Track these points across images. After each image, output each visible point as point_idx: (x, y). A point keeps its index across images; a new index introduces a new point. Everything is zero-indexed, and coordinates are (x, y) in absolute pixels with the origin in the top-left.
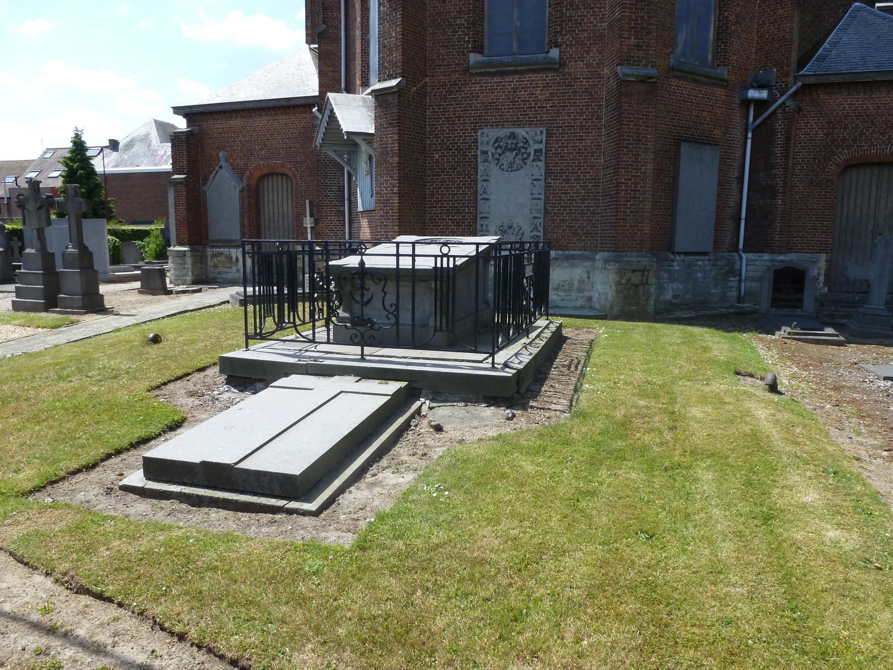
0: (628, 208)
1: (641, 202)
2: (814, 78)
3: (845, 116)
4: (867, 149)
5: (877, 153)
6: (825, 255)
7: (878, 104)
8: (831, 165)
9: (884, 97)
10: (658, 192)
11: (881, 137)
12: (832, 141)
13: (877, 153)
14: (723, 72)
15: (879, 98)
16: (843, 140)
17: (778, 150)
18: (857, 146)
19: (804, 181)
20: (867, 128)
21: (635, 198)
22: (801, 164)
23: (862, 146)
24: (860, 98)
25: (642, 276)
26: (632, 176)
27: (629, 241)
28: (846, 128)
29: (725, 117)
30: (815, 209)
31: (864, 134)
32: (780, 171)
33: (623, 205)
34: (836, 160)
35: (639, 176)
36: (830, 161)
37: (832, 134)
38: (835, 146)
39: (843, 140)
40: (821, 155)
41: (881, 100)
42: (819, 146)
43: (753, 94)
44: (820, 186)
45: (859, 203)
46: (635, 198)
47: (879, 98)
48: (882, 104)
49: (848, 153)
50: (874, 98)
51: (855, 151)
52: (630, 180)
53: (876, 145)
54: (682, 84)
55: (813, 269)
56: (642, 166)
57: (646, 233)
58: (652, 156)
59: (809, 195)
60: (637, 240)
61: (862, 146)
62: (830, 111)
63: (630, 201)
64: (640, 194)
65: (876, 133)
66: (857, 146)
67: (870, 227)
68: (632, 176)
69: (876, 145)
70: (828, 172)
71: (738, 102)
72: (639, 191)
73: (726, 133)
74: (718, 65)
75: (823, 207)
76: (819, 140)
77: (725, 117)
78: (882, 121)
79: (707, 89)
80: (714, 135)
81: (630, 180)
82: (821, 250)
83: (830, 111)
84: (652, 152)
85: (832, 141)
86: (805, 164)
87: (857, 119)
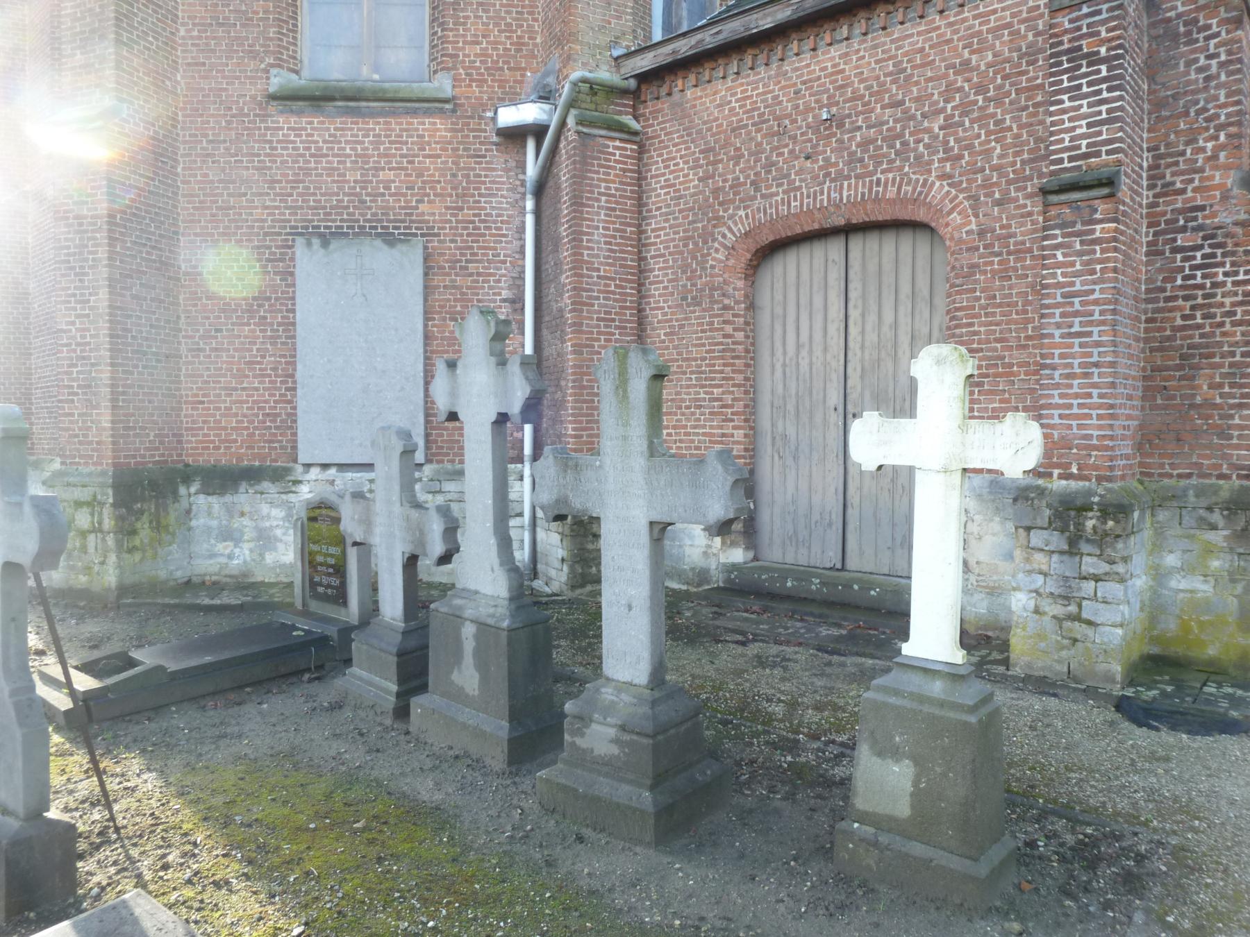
0: (73, 380)
1: (93, 365)
2: (651, 55)
3: (733, 130)
4: (783, 199)
5: (802, 205)
7: (795, 84)
8: (717, 250)
9: (808, 65)
10: (255, 343)
11: (808, 164)
12: (716, 191)
13: (802, 205)
14: (443, 85)
15: (797, 69)
16: (736, 185)
17: (563, 230)
18: (763, 196)
19: (672, 294)
20: (777, 148)
21: (84, 358)
22: (663, 255)
23: (773, 195)
24: (756, 82)
25: (92, 515)
26: (78, 316)
27: (80, 443)
28: (737, 158)
29: (454, 175)
30: (695, 359)
31: (773, 164)
32: (567, 277)
33: (66, 373)
34: (724, 236)
35: (88, 316)
36: (714, 240)
37: (713, 177)
38: (720, 204)
39: (736, 185)
40: (695, 229)
41: (802, 75)
42: (692, 209)
43: (509, 116)
44: (699, 304)
46: (84, 358)
47: (797, 69)
48: (804, 83)
49: (747, 215)
50: (787, 71)
51: (759, 209)
52: (73, 323)
53: (800, 188)
54: (311, 123)
56: (90, 294)
57: (104, 429)
58: (104, 273)
59: (682, 326)
60: (91, 443)
61: (773, 195)
62: (705, 123)
63: (75, 365)
64: (91, 350)
65: (797, 158)
66: (763, 196)
67: (834, 398)
68: (78, 316)
69: (800, 188)
70: (713, 267)
71: (495, 139)
72: (89, 344)
73: (461, 209)
74: (435, 72)
75: (707, 352)
76: (692, 195)
77: (454, 175)
78: (808, 126)
79: (386, 123)
80: (423, 214)
81: (73, 323)
83: (705, 123)
84: (106, 266)
85: (716, 191)
86: (670, 254)
87: (758, 131)
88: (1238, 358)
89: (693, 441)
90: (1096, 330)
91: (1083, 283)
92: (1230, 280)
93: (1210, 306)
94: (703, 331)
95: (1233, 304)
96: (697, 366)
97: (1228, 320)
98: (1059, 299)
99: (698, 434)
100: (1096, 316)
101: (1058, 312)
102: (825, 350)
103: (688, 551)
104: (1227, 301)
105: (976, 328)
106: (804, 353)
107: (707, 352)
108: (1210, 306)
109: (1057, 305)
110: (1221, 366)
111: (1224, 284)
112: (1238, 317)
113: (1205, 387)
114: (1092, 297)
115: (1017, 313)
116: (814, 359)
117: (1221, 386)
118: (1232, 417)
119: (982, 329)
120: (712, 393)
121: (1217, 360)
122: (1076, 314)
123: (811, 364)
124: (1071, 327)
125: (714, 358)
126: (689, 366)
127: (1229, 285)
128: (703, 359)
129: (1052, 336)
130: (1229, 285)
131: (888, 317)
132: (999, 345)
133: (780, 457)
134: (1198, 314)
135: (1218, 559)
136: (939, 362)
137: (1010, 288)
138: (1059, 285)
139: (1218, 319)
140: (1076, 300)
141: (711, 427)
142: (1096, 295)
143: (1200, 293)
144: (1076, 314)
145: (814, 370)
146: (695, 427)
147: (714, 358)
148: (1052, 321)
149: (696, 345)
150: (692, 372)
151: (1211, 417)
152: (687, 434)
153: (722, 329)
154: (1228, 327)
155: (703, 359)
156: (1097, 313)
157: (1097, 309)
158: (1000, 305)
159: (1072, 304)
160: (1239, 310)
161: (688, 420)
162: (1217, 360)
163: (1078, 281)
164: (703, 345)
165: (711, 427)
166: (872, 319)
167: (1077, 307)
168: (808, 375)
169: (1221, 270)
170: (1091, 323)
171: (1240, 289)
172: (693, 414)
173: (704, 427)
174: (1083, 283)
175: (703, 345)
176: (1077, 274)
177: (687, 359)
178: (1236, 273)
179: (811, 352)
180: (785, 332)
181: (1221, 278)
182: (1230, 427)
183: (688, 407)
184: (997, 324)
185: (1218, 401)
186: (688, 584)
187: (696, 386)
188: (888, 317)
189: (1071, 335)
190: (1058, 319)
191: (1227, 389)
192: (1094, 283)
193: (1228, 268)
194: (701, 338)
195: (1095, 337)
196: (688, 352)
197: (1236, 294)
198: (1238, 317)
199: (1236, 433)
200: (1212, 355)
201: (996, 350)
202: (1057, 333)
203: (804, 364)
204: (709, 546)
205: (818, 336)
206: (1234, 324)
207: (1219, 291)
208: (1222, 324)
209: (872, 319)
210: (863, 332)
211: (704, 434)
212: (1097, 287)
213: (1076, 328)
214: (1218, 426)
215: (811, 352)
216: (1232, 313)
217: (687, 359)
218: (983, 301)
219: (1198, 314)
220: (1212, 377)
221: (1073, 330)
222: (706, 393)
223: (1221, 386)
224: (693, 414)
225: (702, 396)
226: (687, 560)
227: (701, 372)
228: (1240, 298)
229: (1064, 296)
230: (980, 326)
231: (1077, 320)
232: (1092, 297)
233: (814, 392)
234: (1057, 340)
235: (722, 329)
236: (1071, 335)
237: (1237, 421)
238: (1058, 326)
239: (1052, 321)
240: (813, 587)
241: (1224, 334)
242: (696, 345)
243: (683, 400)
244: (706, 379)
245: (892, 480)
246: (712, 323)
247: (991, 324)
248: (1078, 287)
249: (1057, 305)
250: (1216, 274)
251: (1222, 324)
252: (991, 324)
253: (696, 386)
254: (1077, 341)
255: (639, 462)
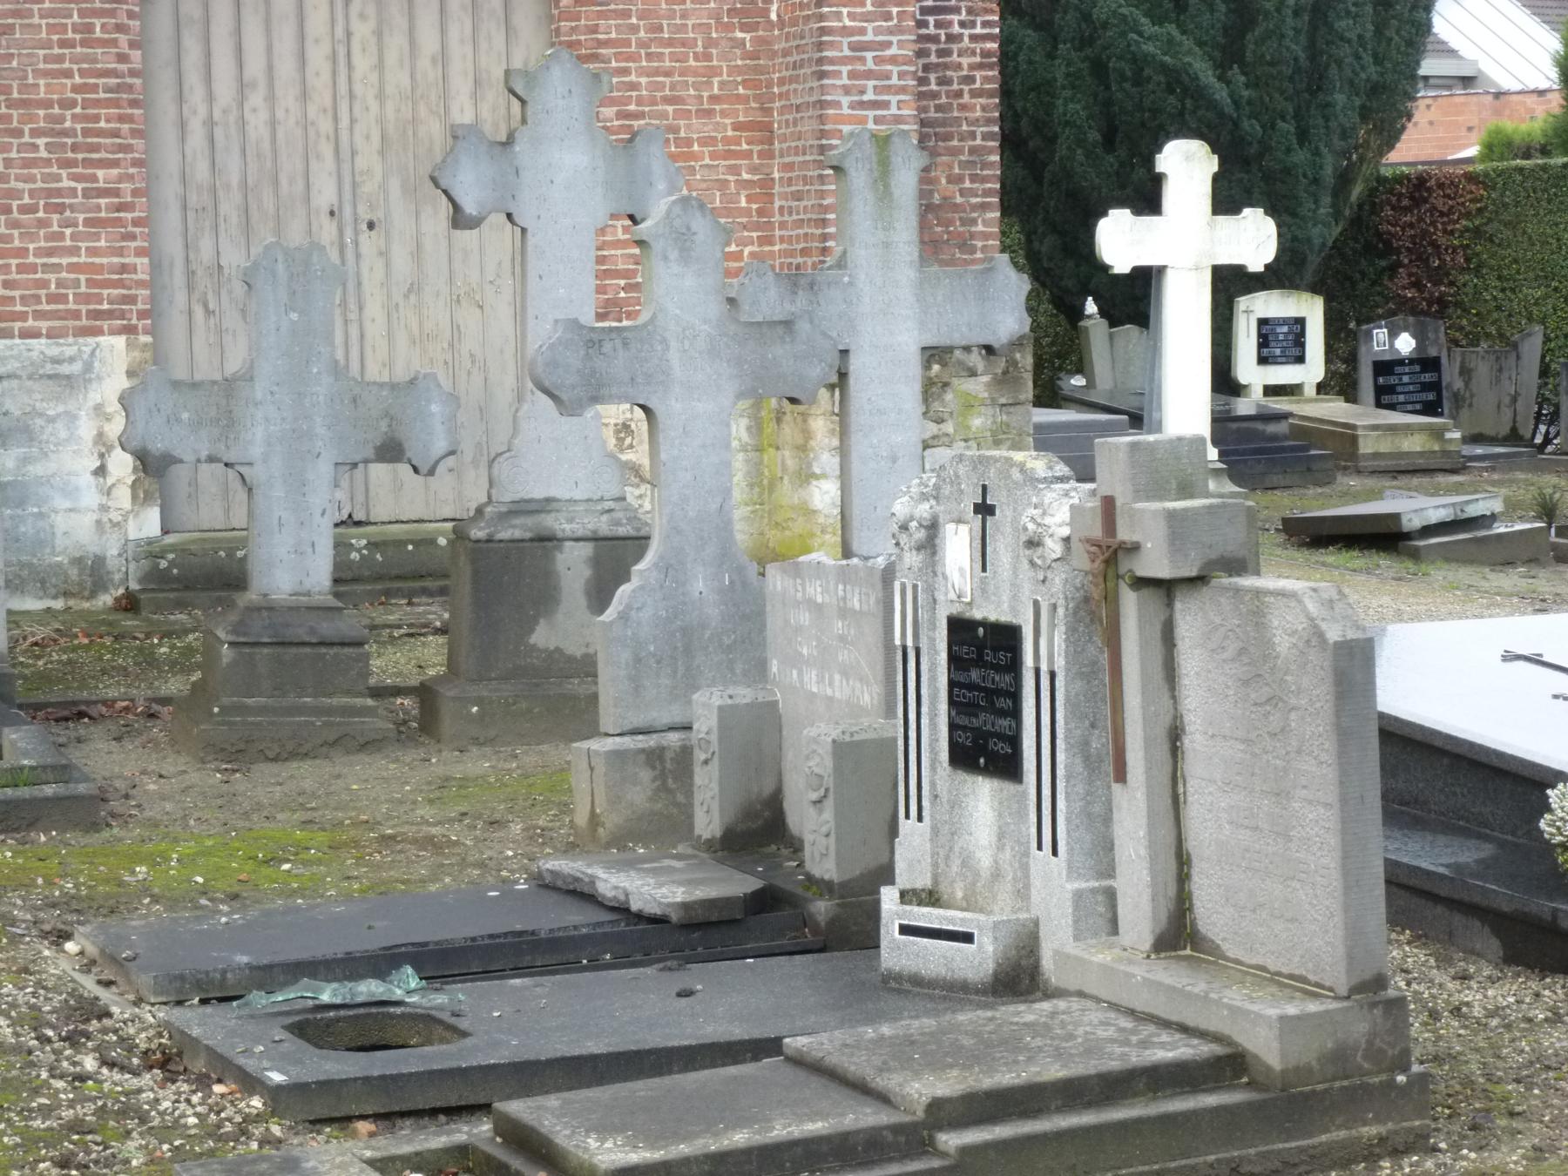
6: (120, 341)
30: (47, 104)
45: (255, 66)
55: (72, 417)
75: (76, 89)
82: (96, 315)
88: (978, 142)
89: (44, 284)
90: (894, 99)
91: (877, 31)
92: (967, 32)
93: (946, 66)
94: (63, 44)
95: (972, 67)
96: (50, 118)
97: (966, 88)
98: (847, 52)
99: (57, 268)
100: (895, 81)
101: (845, 69)
102: (304, 96)
103: (61, 523)
104: (965, 61)
105: (633, 78)
106: (256, 99)
107: (76, 89)
108: (946, 66)
109: (844, 61)
110: (959, 151)
111: (959, 37)
112: (978, 85)
113: (944, 181)
114: (888, 52)
115: (696, 59)
116: (280, 114)
117: (960, 179)
118: (974, 222)
119: (643, 80)
120: (94, 179)
121: (955, 143)
122: (869, 75)
123: (273, 123)
124: (862, 92)
125: (97, 103)
126: (32, 119)
127: (966, 39)
128: (68, 104)
129: (838, 104)
130: (966, 39)
131: (429, 41)
132: (670, 109)
133: (208, 312)
134: (932, 77)
135: (980, 414)
136: (1188, 158)
137: (684, 16)
138: (845, 31)
139: (955, 87)
140: (869, 55)
141: (92, 252)
142: (893, 51)
143: (933, 47)
144: (869, 75)
145: (280, 135)
146: (50, 252)
147: (97, 103)
148: (838, 82)
149: (47, 74)
150: (36, 133)
151: (950, 222)
152: (33, 268)
153: (114, 43)
154: (966, 98)
155: (68, 104)
156: (895, 76)
157: (895, 69)
158: (670, 43)
159: (863, 60)
160: (978, 75)
161: (32, 237)
162: (955, 143)
163: (870, 27)
164: (68, 74)
165: (92, 252)
166: (396, 43)
167: (870, 65)
168: (266, 145)
169: (955, 18)
170: (888, 89)
171: (978, 46)
172: (42, 223)
173: (75, 251)
174: (877, 31)
175: (68, 74)
176: (867, 18)
177: (24, 103)
178: (973, 24)
179: (271, 98)
180: (208, 54)
181: (956, 29)
182: (972, 236)
183: (24, 209)
184: (668, 74)
185: (959, 200)
186: (67, 594)
187: (48, 162)
188: (429, 41)
189: (862, 105)
190: (845, 81)
191: (967, 184)
192: (890, 32)
193: (963, 16)
194: (60, 59)
195: (894, 110)
196: (24, 88)
197: (973, 53)
198: (978, 85)
199: (980, 244)
200: (947, 137)
201: (664, 115)
202: (845, 101)
203: (257, 123)
204: (104, 508)
205: (286, 67)
206: (974, 94)
207: (955, 47)
208: (959, 94)
209: (396, 43)
210: (380, 66)
211: (73, 268)
212: (894, 39)
213: (869, 96)
214: (960, 234)
215: (271, 98)
216: (969, 80)
217: (24, 103)
218: (642, 34)
219: (932, 77)
220: (951, 167)
221: (865, 98)
222: (76, 178)
223: (960, 179)
224: (42, 223)
225: (66, 183)
226: (60, 542)
227: (65, 133)
228: (978, 59)
229: (854, 47)
230: (639, 75)
231: (871, 83)
232: (888, 52)
233: (284, 181)
234: (846, 111)
235: (114, 43)
236: (862, 105)
237: (980, 228)
238: (847, 90)
239: (838, 82)
240: (354, 556)
241: (963, 107)
242: (47, 74)
243: (16, 194)
244: (75, 147)
245: (451, 345)
246: (89, 28)
247: (657, 72)
248: (869, 37)
249: (844, 61)
250: (950, 23)
251: (959, 94)
252: (657, 72)
253: (48, 162)
254: (871, 114)
255: (905, 269)
